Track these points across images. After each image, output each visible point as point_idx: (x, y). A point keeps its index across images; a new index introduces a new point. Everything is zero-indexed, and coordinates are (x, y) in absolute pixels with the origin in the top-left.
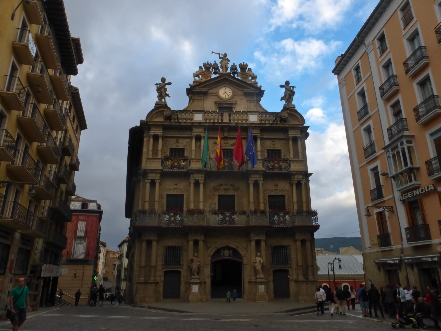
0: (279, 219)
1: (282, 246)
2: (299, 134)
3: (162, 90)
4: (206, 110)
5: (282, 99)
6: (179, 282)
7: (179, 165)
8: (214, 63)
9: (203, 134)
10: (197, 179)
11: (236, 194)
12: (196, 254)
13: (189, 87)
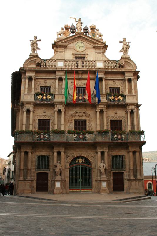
0: (117, 137)
1: (119, 156)
2: (133, 76)
3: (34, 45)
4: (66, 59)
5: (121, 51)
6: (47, 180)
7: (47, 98)
8: (72, 25)
9: (64, 76)
10: (60, 108)
11: (87, 119)
12: (59, 162)
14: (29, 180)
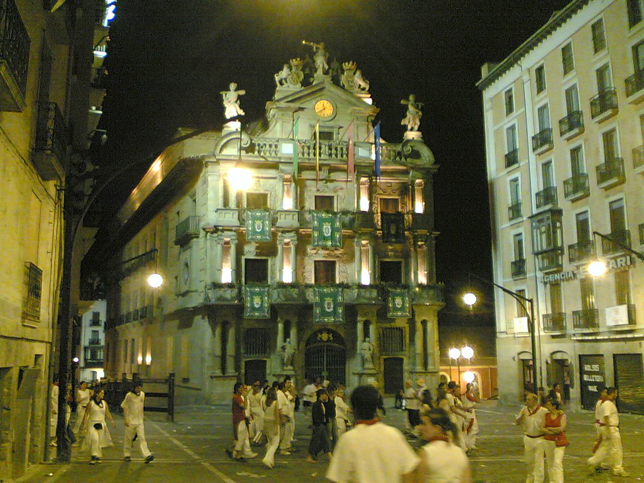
14: (232, 375)
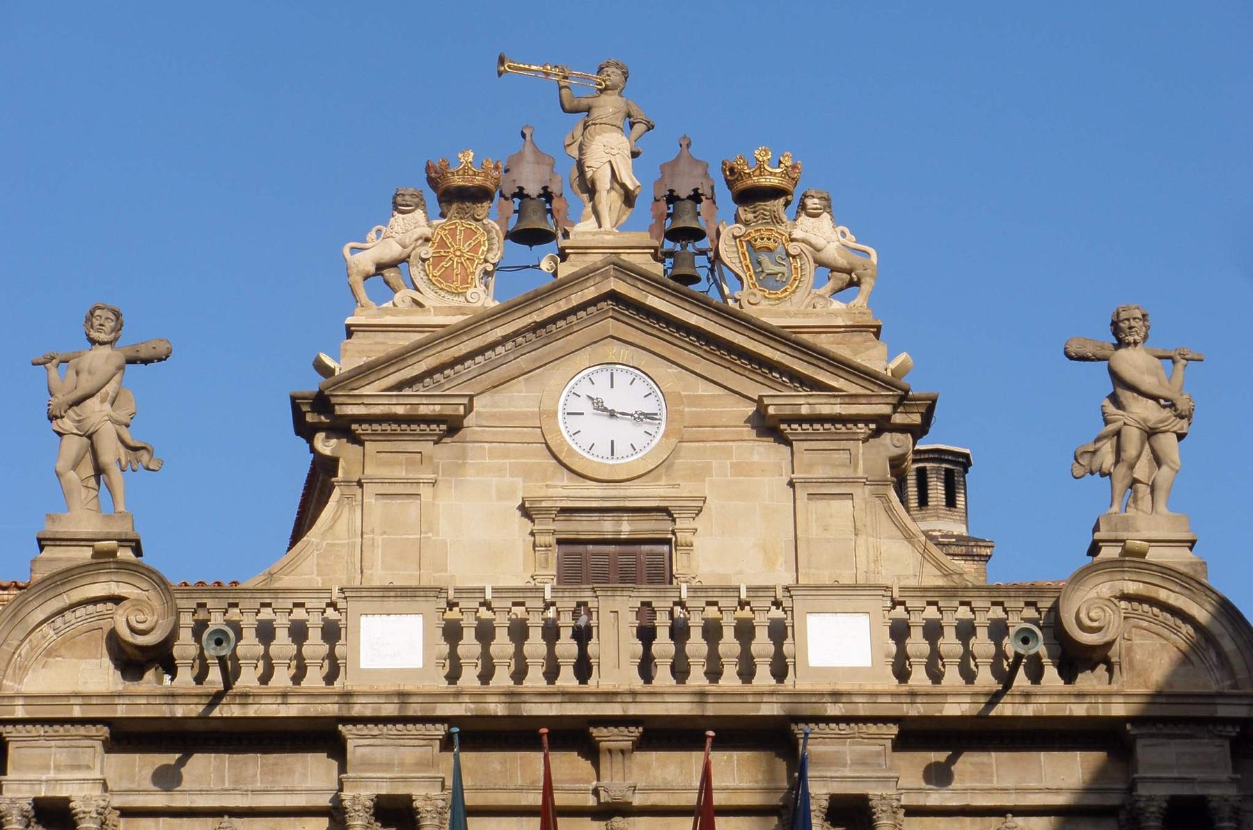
13: (312, 384)
